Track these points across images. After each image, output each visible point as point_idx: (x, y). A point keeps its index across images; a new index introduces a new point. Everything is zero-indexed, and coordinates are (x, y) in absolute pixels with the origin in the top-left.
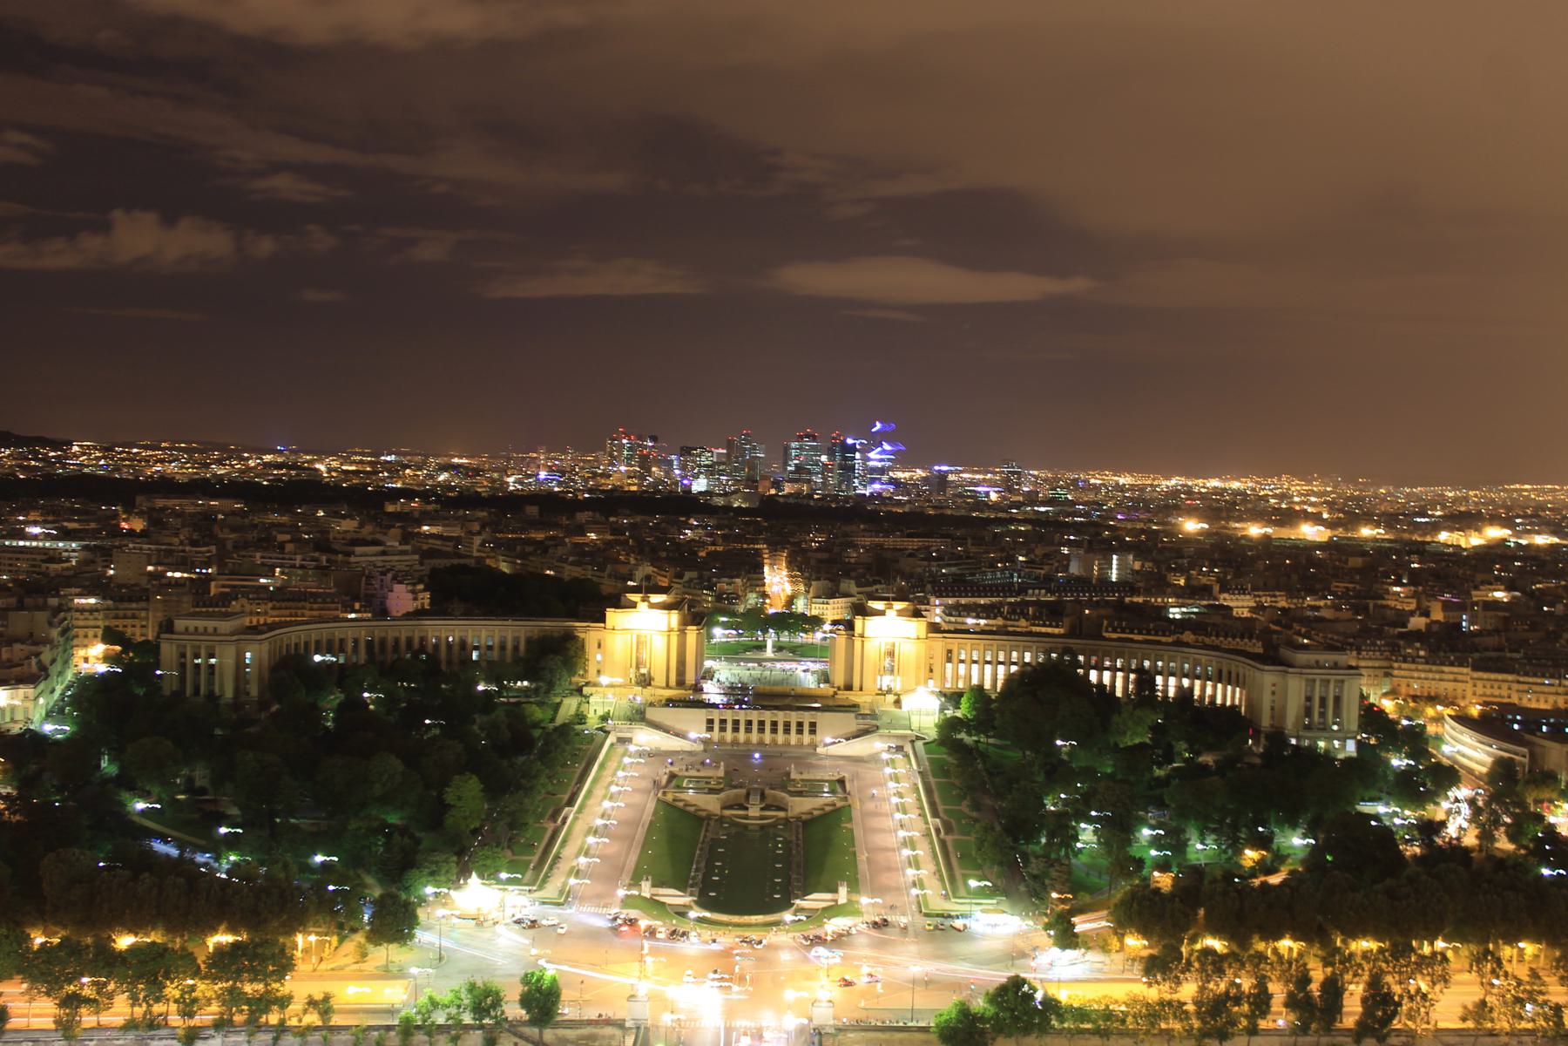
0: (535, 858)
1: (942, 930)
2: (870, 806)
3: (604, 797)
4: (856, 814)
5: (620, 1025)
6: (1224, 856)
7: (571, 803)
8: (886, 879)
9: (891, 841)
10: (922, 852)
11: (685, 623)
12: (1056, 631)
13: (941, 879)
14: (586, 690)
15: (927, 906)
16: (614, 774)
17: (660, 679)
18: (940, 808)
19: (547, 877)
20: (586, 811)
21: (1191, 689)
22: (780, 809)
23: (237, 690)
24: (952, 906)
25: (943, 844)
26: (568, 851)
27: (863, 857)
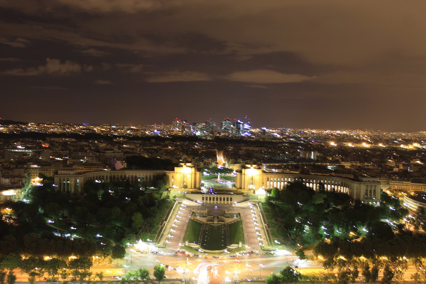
0: (156, 235)
1: (268, 253)
2: (248, 220)
3: (175, 218)
4: (244, 223)
5: (181, 280)
6: (344, 234)
7: (166, 220)
8: (252, 240)
9: (253, 230)
12: (297, 172)
13: (267, 240)
14: (169, 189)
16: (177, 212)
17: (189, 186)
18: (266, 221)
19: (160, 240)
20: (170, 222)
21: (334, 189)
22: (222, 221)
23: (75, 190)
24: (270, 248)
25: (267, 231)
26: (165, 233)
27: (245, 234)
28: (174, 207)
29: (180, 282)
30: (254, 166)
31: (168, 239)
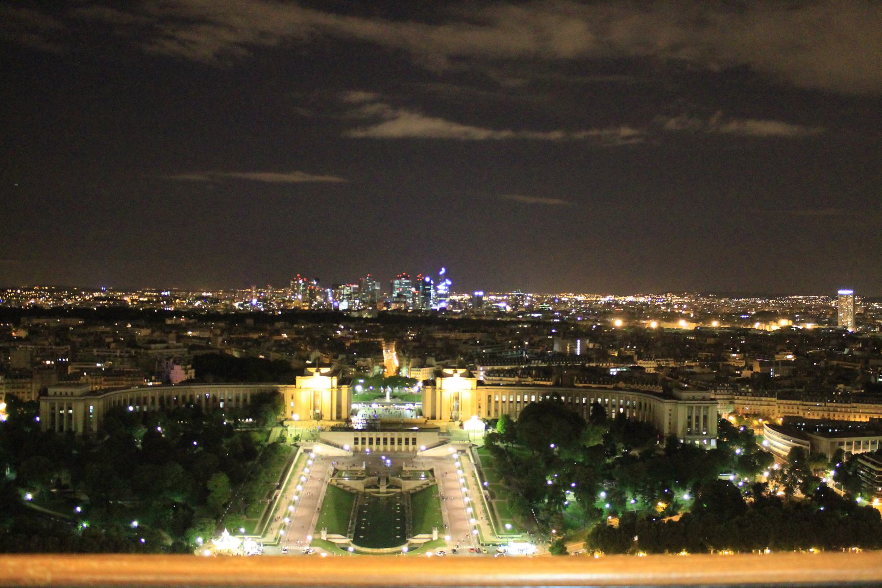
0: (260, 520)
3: (298, 484)
6: (647, 507)
7: (279, 487)
8: (459, 525)
10: (479, 508)
11: (341, 383)
12: (548, 383)
13: (490, 524)
14: (285, 423)
15: (483, 540)
16: (303, 470)
17: (327, 416)
19: (267, 529)
23: (85, 427)
25: (490, 505)
26: (280, 514)
27: (445, 513)
31: (284, 527)
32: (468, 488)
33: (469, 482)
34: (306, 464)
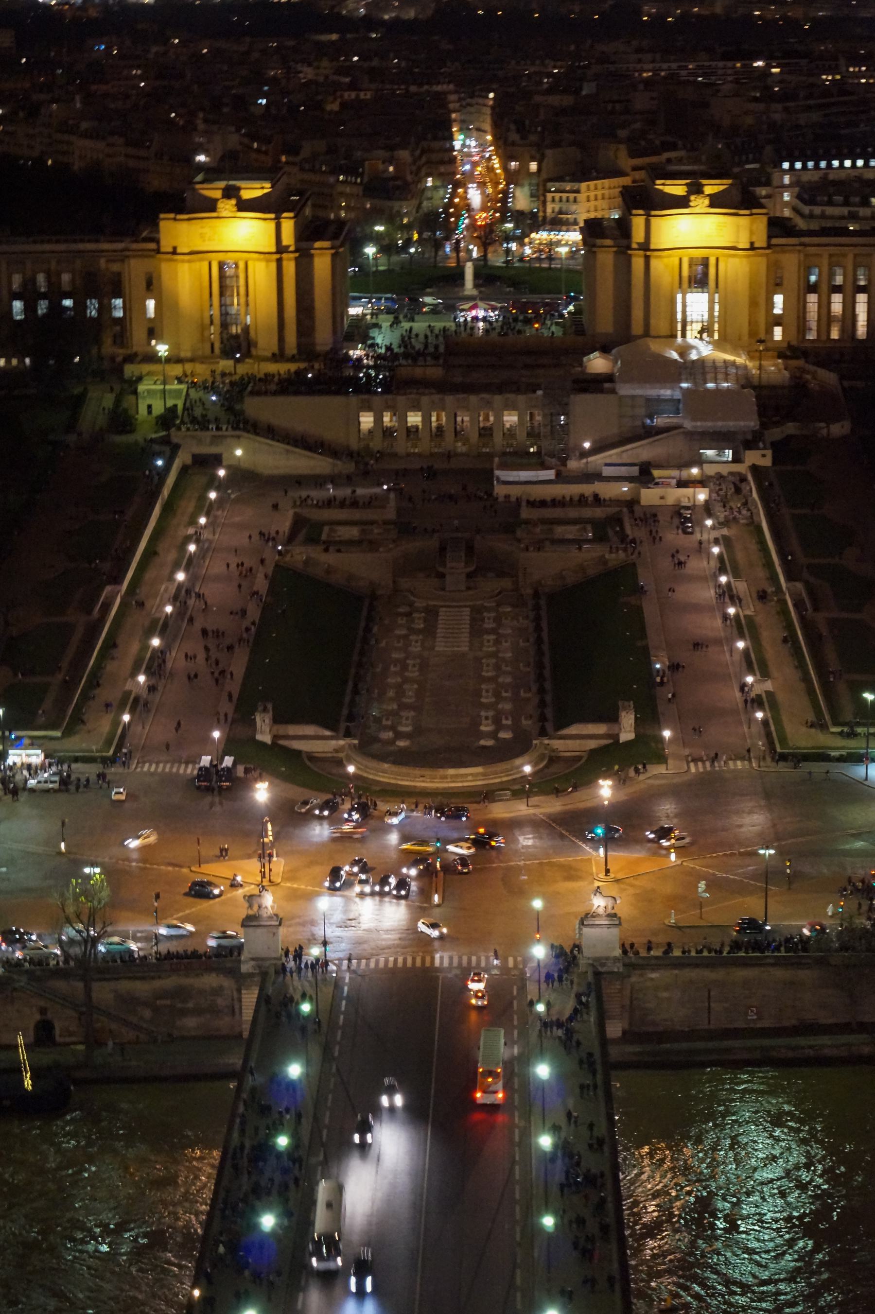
7: (117, 580)
11: (308, 234)
14: (130, 370)
15: (783, 740)
16: (193, 521)
17: (266, 343)
28: (166, 492)
29: (227, 983)
30: (711, 187)
32: (736, 574)
33: (740, 556)
34: (203, 497)
